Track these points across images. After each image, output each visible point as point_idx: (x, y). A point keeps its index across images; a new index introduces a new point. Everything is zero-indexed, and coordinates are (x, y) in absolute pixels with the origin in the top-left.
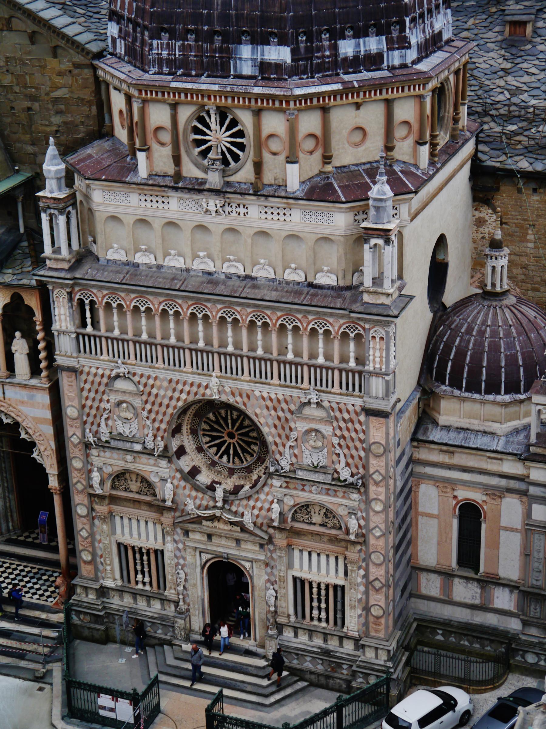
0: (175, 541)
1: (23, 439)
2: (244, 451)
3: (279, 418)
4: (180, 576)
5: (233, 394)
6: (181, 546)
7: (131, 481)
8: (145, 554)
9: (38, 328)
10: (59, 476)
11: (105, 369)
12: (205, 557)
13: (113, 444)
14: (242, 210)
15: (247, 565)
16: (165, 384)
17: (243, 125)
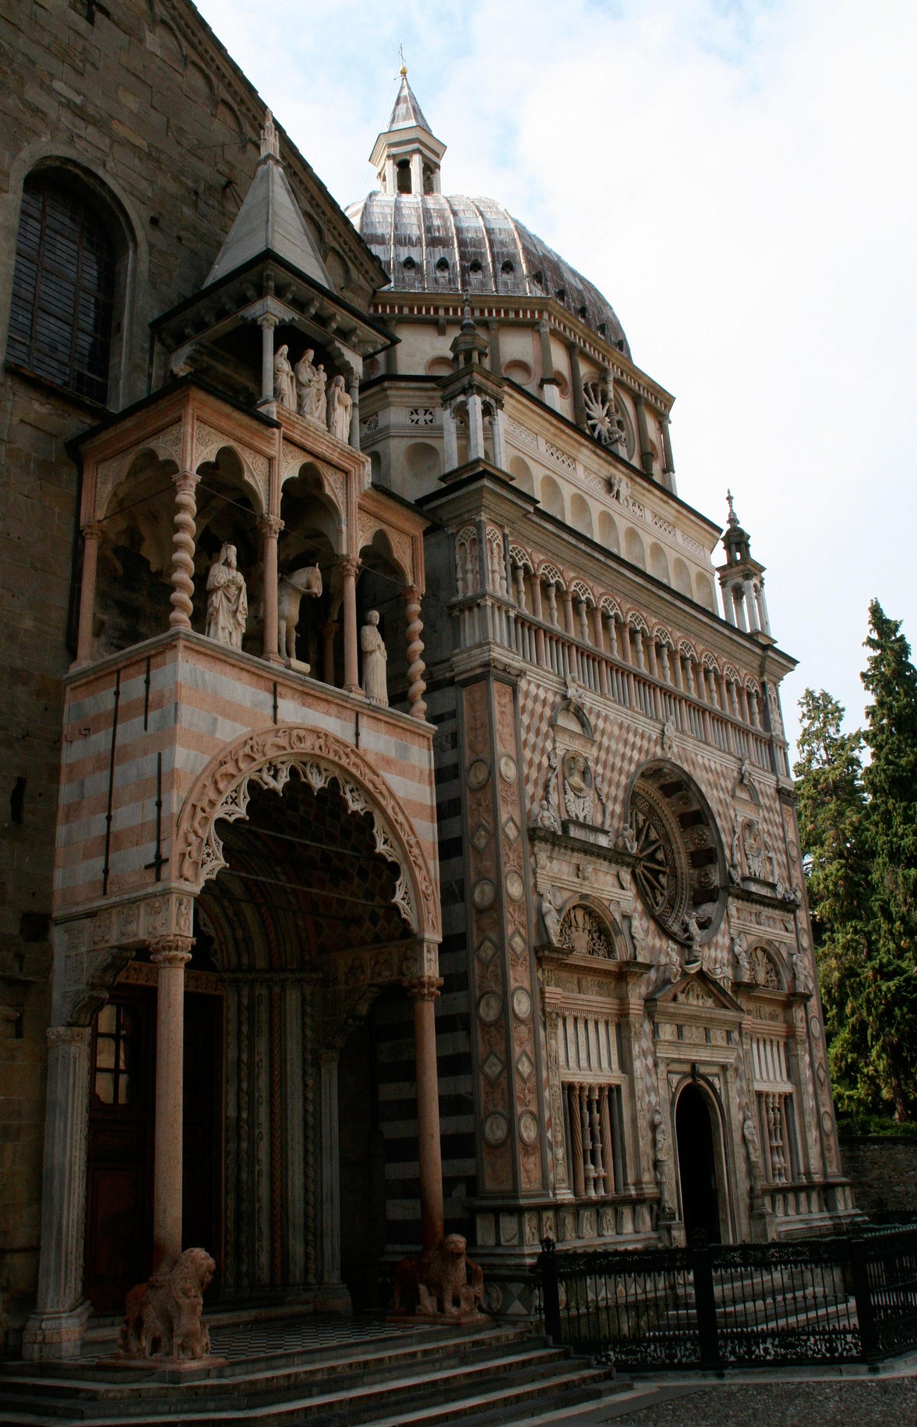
0: (644, 1054)
1: (380, 855)
2: (653, 888)
3: (721, 801)
4: (662, 1126)
5: (680, 758)
6: (650, 1062)
7: (577, 927)
8: (595, 1106)
9: (416, 607)
10: (441, 946)
11: (547, 690)
12: (675, 1079)
13: (574, 832)
14: (636, 509)
15: (717, 1082)
16: (616, 730)
17: (625, 413)
